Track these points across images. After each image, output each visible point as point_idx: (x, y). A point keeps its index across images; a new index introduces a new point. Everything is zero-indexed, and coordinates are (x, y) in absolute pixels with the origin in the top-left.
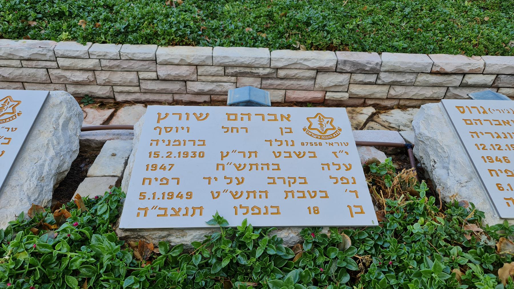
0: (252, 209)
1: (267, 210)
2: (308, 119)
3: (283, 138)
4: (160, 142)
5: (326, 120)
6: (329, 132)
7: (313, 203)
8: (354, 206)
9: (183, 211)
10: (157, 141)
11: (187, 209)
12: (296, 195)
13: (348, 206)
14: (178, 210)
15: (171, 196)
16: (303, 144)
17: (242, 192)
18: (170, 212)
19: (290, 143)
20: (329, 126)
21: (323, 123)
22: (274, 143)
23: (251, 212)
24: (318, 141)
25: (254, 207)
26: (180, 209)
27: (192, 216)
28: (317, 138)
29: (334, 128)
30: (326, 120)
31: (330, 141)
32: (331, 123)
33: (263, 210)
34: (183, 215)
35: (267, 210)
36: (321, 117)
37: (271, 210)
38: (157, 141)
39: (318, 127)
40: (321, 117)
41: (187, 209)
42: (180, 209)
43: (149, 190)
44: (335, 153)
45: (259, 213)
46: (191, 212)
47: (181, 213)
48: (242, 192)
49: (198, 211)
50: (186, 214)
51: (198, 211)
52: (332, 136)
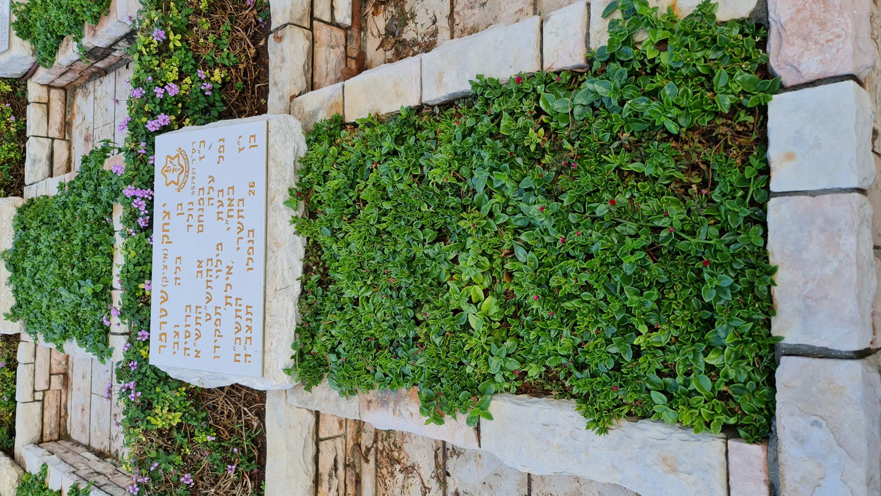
0: (249, 254)
2: (167, 185)
3: (187, 213)
4: (187, 346)
5: (169, 164)
6: (182, 162)
10: (186, 349)
11: (247, 319)
12: (241, 208)
16: (193, 193)
19: (190, 206)
20: (175, 162)
23: (251, 256)
24: (190, 176)
29: (177, 156)
30: (169, 164)
31: (190, 160)
32: (173, 159)
33: (251, 244)
37: (251, 238)
38: (186, 349)
39: (176, 173)
41: (247, 319)
44: (201, 158)
45: (252, 248)
46: (249, 316)
49: (249, 310)
50: (251, 319)
52: (186, 159)
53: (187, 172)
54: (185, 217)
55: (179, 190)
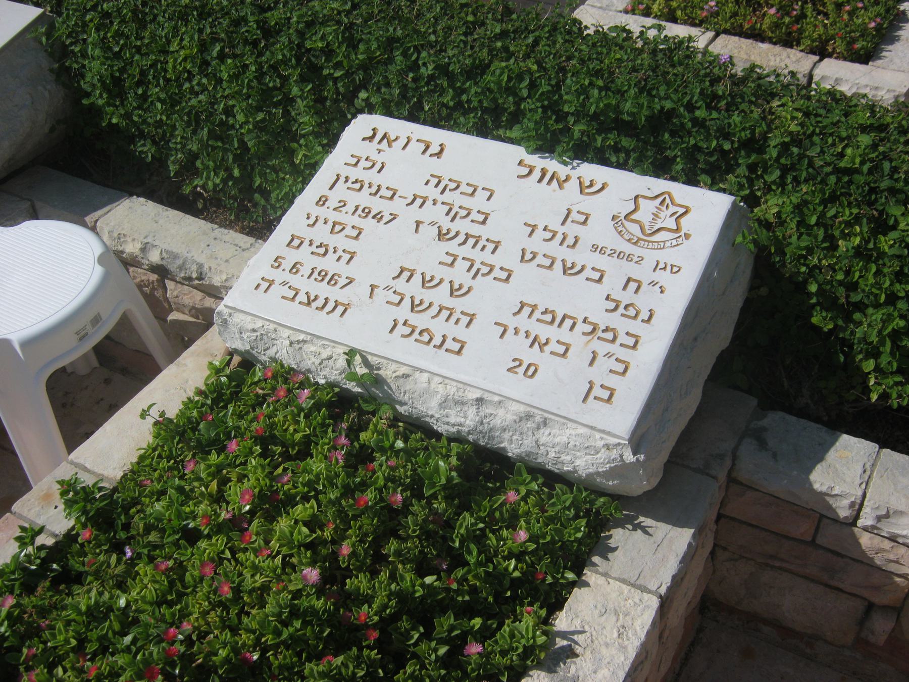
1: (443, 342)
5: (673, 209)
7: (531, 355)
8: (602, 386)
9: (320, 302)
13: (590, 382)
14: (312, 298)
15: (323, 275)
17: (431, 304)
18: (302, 297)
21: (662, 215)
22: (539, 231)
25: (426, 330)
26: (316, 298)
27: (328, 313)
28: (629, 240)
34: (317, 308)
35: (443, 342)
36: (668, 201)
40: (668, 201)
42: (316, 298)
43: (292, 256)
47: (314, 305)
48: (431, 304)
51: (340, 309)
53: (635, 244)
54: (555, 225)
55: (614, 218)
